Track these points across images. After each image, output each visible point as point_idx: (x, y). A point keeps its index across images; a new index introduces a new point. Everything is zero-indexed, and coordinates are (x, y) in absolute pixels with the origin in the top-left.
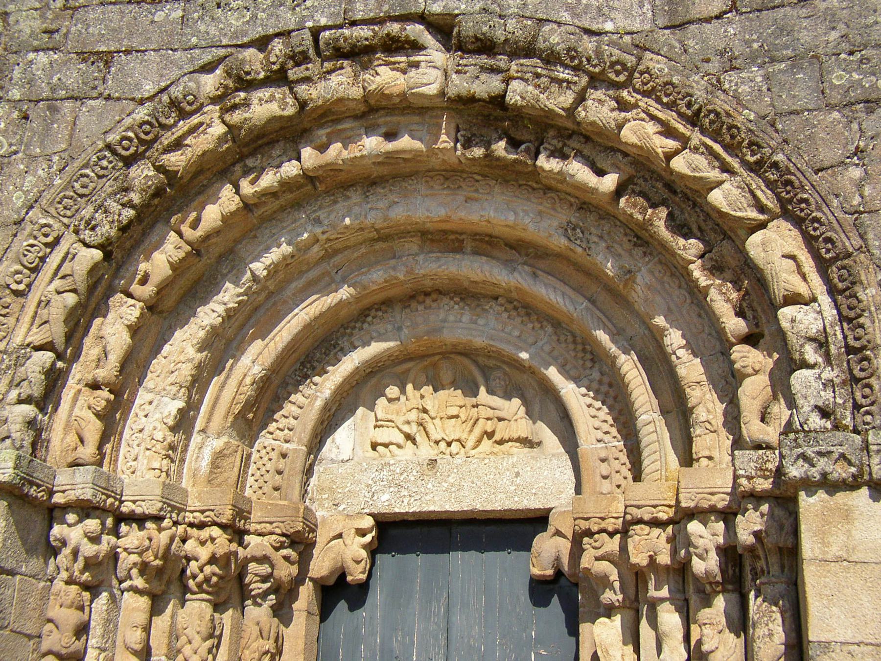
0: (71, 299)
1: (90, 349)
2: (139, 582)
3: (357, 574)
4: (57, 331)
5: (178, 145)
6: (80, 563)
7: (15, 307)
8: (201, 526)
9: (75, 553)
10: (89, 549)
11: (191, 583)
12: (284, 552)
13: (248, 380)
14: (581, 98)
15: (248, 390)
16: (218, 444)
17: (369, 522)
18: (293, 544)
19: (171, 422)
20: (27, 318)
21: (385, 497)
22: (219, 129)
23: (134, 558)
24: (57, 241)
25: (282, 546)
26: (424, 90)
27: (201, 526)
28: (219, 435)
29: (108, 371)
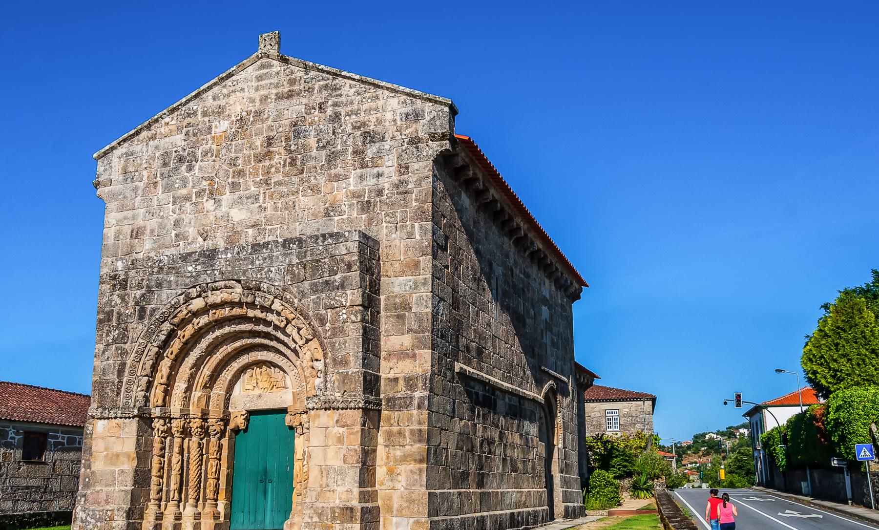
0: (151, 362)
1: (158, 375)
2: (178, 435)
3: (242, 427)
4: (148, 371)
5: (175, 317)
6: (160, 432)
7: (137, 366)
8: (194, 418)
9: (158, 430)
10: (162, 428)
11: (193, 434)
12: (219, 423)
13: (206, 376)
14: (273, 302)
15: (206, 379)
16: (200, 394)
17: (244, 412)
18: (222, 420)
19: (183, 391)
20: (140, 368)
21: (248, 405)
22: (185, 312)
23: (175, 429)
24: (146, 346)
25: (218, 422)
26: (235, 300)
27: (194, 418)
28: (199, 392)
29: (164, 380)
